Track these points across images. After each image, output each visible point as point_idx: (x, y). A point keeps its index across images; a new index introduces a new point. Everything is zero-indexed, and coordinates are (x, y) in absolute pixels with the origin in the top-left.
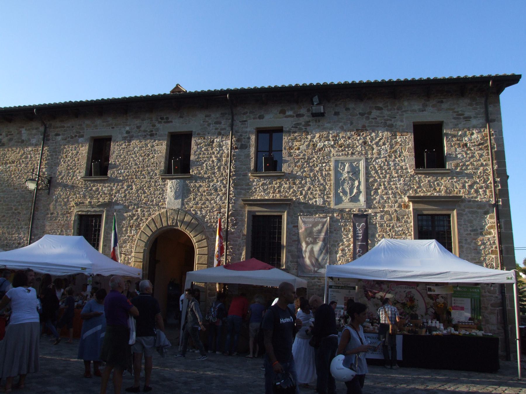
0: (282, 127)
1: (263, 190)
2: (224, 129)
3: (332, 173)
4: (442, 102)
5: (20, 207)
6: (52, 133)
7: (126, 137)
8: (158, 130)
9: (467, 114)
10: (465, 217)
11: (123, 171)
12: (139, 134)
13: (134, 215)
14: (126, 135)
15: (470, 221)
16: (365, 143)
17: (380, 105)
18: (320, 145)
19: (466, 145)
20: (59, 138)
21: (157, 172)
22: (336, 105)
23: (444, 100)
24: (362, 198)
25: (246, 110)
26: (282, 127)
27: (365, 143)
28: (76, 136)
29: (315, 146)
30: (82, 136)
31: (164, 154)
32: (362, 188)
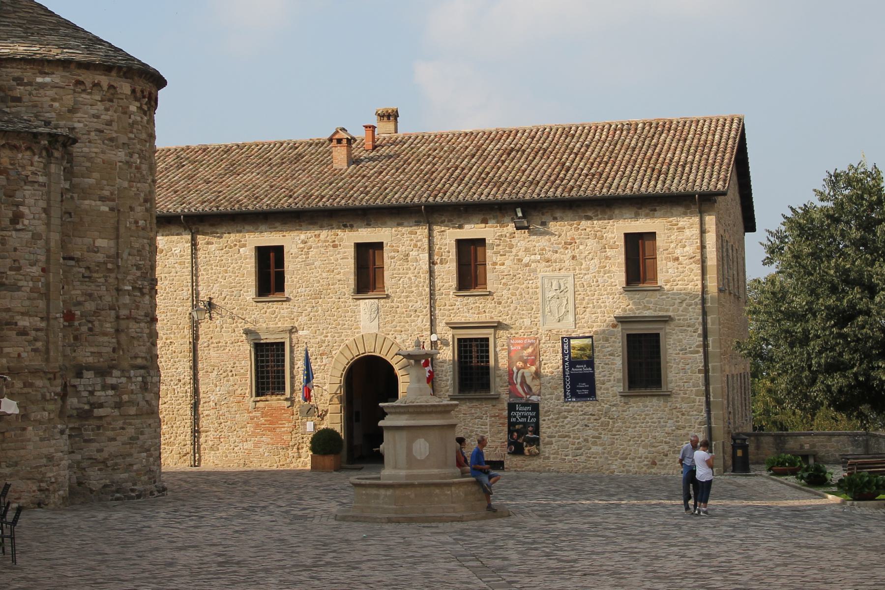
0: (484, 239)
1: (468, 310)
2: (421, 240)
3: (539, 291)
4: (655, 210)
5: (172, 336)
6: (200, 239)
7: (302, 249)
8: (341, 240)
9: (681, 224)
10: (675, 337)
11: (303, 290)
12: (319, 244)
13: (324, 342)
14: (302, 246)
15: (680, 341)
16: (574, 257)
17: (590, 214)
18: (526, 260)
19: (677, 259)
20: (212, 248)
21: (346, 290)
22: (543, 214)
23: (658, 208)
24: (571, 318)
25: (443, 218)
26: (484, 239)
27: (574, 257)
28: (235, 245)
29: (520, 260)
30: (244, 246)
31: (353, 270)
32: (571, 307)
